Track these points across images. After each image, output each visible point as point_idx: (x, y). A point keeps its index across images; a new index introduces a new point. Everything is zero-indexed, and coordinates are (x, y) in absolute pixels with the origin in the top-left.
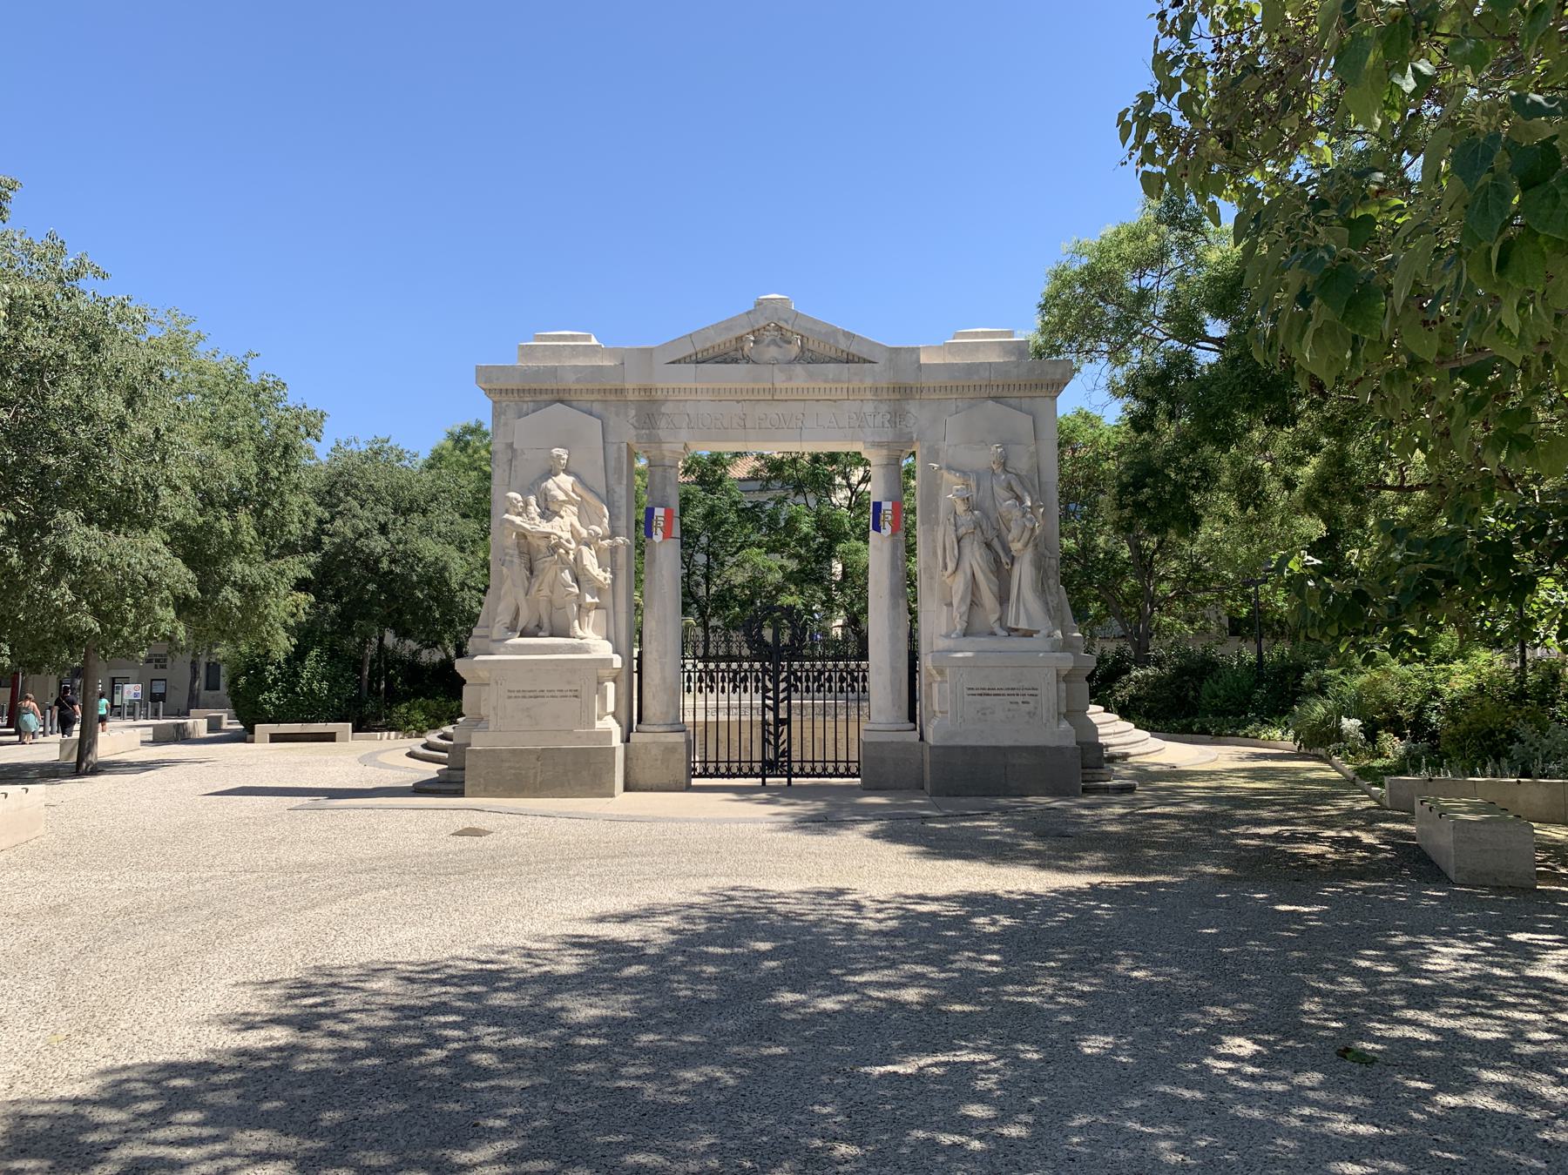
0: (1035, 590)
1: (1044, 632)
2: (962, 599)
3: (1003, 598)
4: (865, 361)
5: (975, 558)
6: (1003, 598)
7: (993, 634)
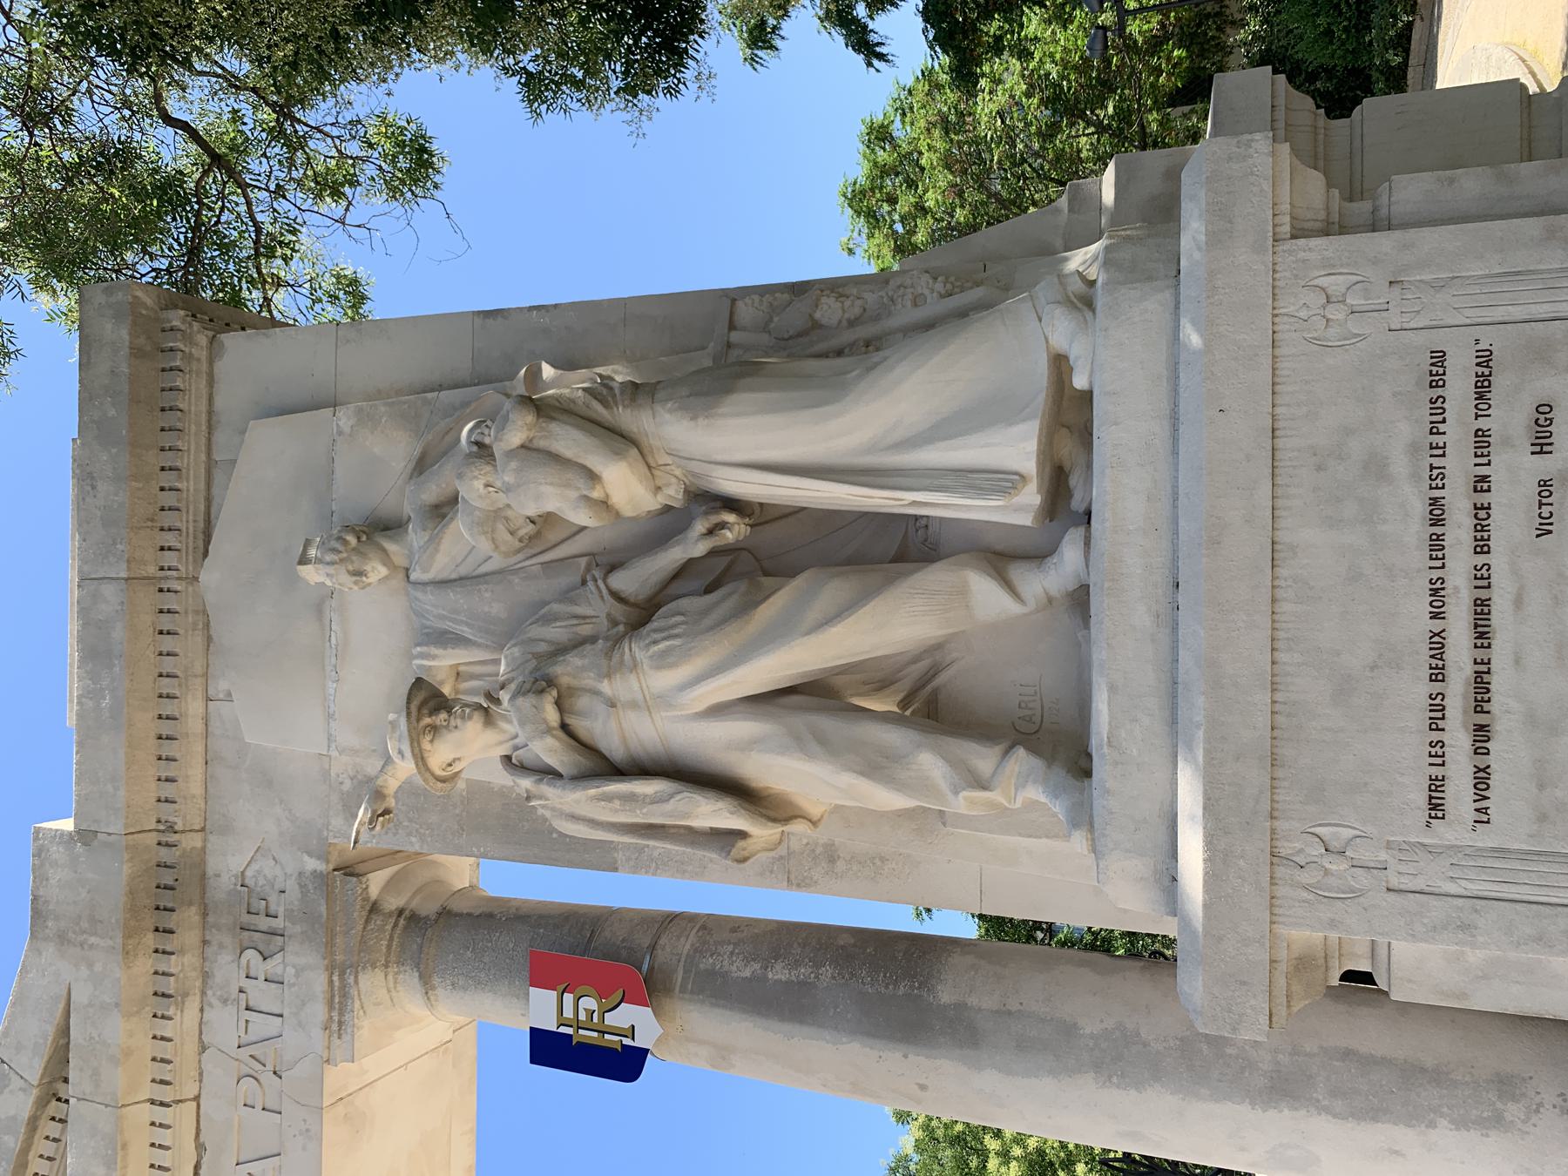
0: (832, 390)
1: (1061, 331)
2: (877, 767)
3: (903, 547)
5: (676, 695)
7: (1080, 600)
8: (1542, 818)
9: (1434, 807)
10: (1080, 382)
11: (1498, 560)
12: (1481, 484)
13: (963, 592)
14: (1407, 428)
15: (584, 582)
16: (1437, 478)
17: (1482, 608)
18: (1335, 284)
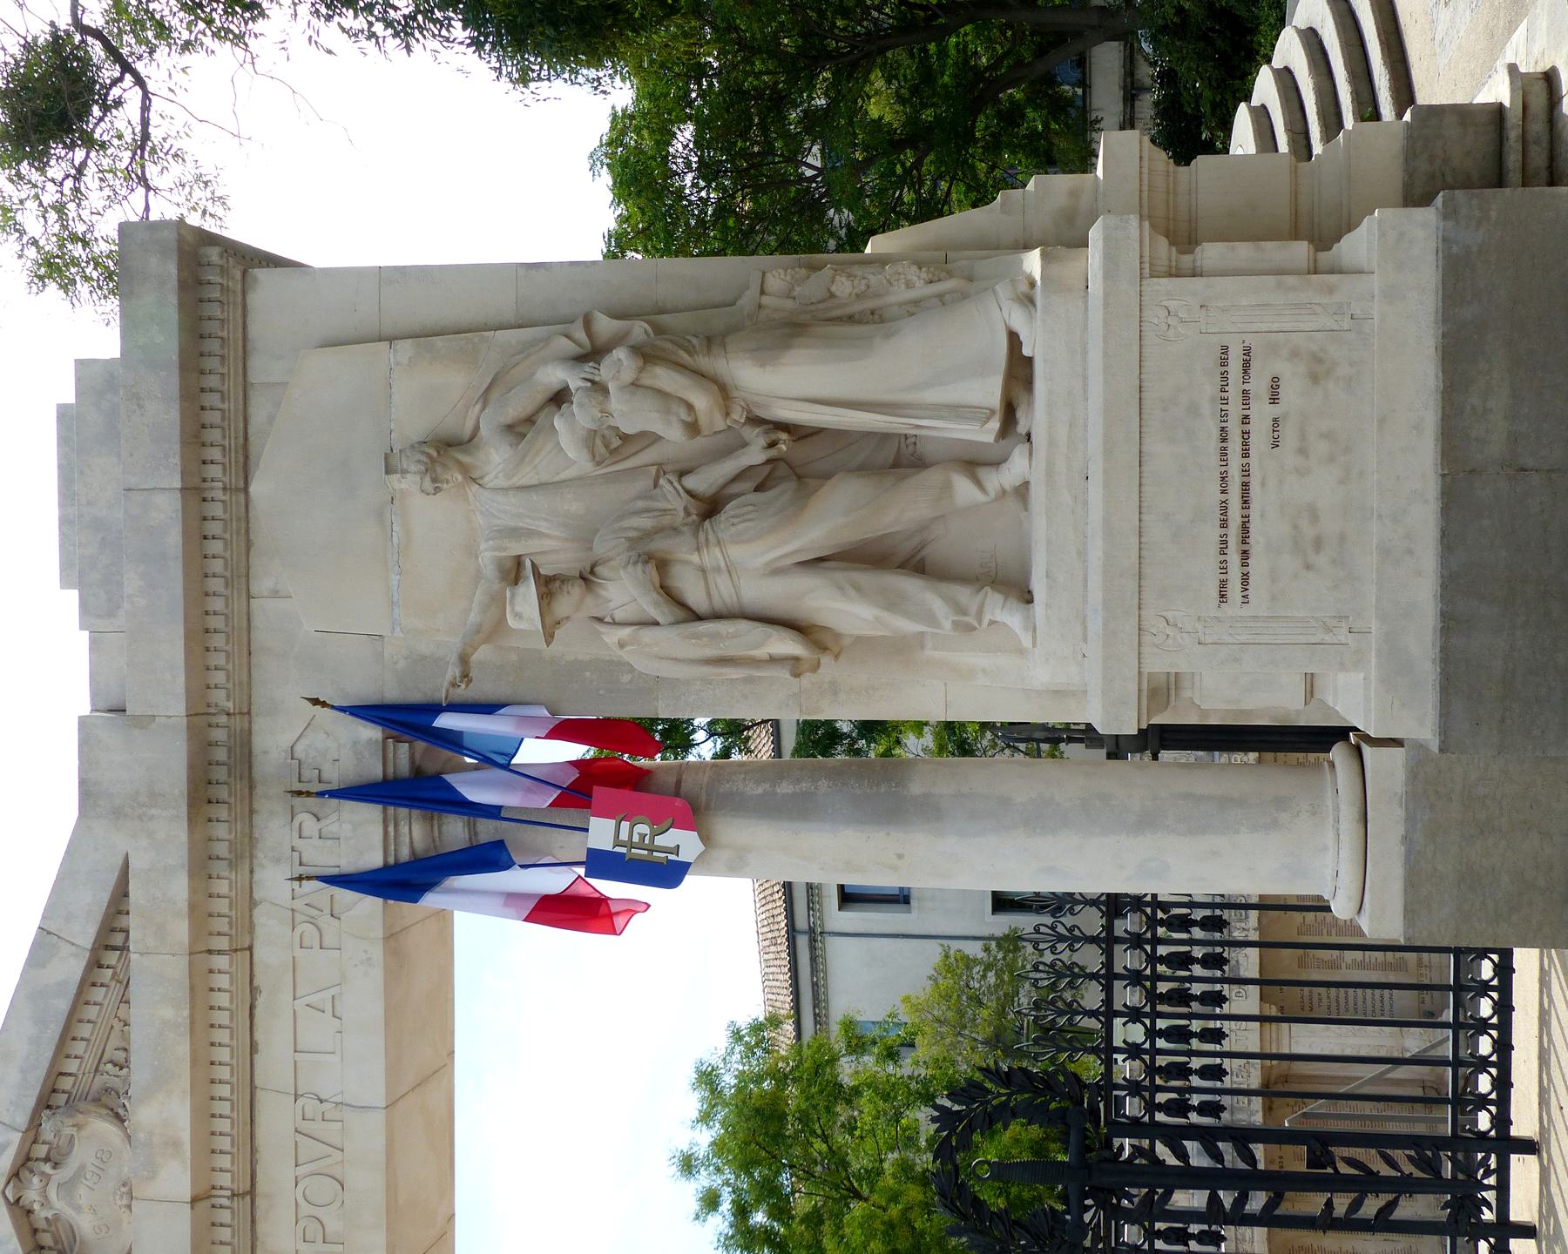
2: (894, 603)
4: (121, 892)
5: (749, 559)
6: (899, 459)
8: (1274, 598)
9: (1222, 596)
10: (1026, 352)
11: (1253, 460)
12: (1246, 419)
13: (947, 487)
14: (1210, 388)
15: (656, 485)
16: (1224, 416)
17: (1245, 487)
18: (1172, 304)
